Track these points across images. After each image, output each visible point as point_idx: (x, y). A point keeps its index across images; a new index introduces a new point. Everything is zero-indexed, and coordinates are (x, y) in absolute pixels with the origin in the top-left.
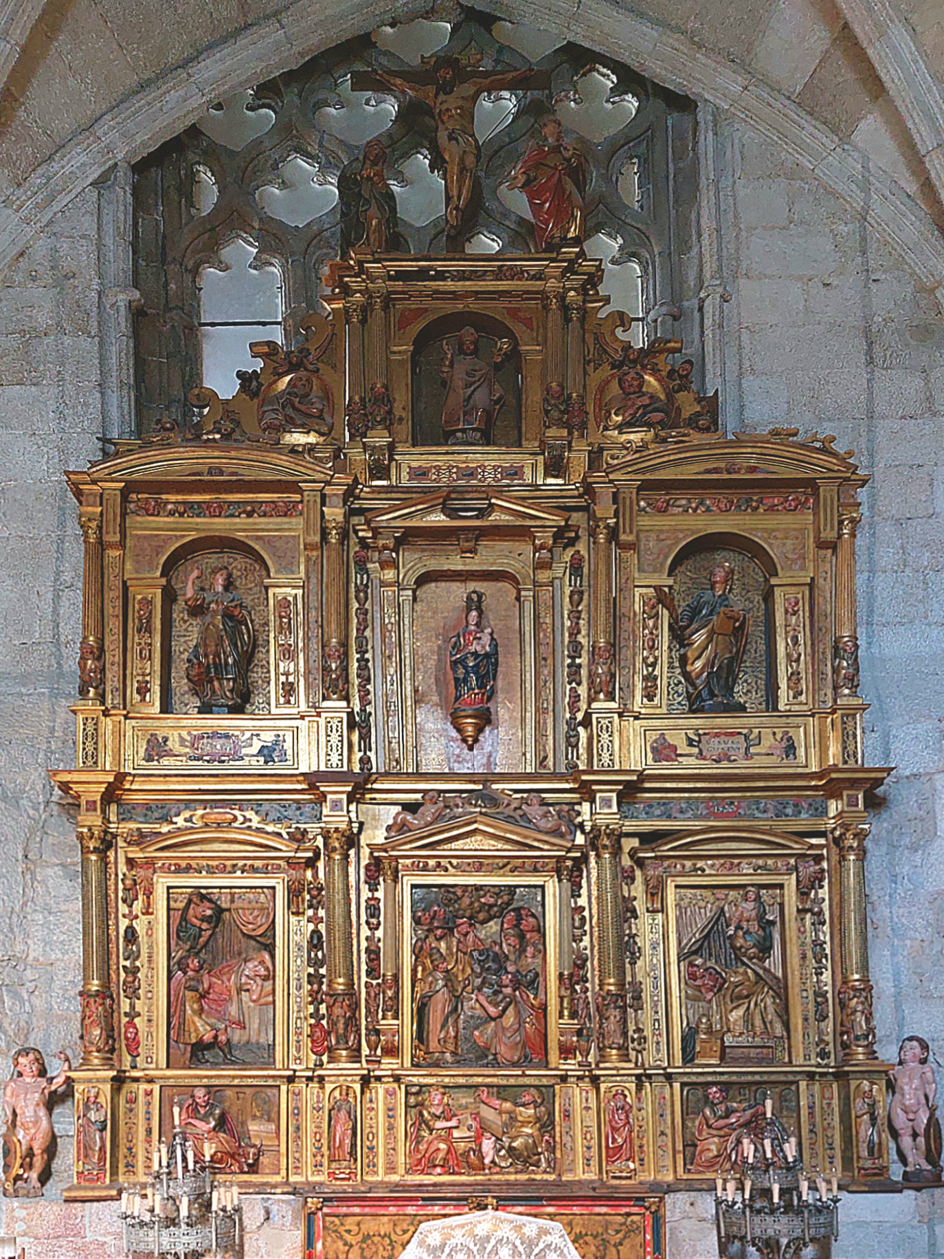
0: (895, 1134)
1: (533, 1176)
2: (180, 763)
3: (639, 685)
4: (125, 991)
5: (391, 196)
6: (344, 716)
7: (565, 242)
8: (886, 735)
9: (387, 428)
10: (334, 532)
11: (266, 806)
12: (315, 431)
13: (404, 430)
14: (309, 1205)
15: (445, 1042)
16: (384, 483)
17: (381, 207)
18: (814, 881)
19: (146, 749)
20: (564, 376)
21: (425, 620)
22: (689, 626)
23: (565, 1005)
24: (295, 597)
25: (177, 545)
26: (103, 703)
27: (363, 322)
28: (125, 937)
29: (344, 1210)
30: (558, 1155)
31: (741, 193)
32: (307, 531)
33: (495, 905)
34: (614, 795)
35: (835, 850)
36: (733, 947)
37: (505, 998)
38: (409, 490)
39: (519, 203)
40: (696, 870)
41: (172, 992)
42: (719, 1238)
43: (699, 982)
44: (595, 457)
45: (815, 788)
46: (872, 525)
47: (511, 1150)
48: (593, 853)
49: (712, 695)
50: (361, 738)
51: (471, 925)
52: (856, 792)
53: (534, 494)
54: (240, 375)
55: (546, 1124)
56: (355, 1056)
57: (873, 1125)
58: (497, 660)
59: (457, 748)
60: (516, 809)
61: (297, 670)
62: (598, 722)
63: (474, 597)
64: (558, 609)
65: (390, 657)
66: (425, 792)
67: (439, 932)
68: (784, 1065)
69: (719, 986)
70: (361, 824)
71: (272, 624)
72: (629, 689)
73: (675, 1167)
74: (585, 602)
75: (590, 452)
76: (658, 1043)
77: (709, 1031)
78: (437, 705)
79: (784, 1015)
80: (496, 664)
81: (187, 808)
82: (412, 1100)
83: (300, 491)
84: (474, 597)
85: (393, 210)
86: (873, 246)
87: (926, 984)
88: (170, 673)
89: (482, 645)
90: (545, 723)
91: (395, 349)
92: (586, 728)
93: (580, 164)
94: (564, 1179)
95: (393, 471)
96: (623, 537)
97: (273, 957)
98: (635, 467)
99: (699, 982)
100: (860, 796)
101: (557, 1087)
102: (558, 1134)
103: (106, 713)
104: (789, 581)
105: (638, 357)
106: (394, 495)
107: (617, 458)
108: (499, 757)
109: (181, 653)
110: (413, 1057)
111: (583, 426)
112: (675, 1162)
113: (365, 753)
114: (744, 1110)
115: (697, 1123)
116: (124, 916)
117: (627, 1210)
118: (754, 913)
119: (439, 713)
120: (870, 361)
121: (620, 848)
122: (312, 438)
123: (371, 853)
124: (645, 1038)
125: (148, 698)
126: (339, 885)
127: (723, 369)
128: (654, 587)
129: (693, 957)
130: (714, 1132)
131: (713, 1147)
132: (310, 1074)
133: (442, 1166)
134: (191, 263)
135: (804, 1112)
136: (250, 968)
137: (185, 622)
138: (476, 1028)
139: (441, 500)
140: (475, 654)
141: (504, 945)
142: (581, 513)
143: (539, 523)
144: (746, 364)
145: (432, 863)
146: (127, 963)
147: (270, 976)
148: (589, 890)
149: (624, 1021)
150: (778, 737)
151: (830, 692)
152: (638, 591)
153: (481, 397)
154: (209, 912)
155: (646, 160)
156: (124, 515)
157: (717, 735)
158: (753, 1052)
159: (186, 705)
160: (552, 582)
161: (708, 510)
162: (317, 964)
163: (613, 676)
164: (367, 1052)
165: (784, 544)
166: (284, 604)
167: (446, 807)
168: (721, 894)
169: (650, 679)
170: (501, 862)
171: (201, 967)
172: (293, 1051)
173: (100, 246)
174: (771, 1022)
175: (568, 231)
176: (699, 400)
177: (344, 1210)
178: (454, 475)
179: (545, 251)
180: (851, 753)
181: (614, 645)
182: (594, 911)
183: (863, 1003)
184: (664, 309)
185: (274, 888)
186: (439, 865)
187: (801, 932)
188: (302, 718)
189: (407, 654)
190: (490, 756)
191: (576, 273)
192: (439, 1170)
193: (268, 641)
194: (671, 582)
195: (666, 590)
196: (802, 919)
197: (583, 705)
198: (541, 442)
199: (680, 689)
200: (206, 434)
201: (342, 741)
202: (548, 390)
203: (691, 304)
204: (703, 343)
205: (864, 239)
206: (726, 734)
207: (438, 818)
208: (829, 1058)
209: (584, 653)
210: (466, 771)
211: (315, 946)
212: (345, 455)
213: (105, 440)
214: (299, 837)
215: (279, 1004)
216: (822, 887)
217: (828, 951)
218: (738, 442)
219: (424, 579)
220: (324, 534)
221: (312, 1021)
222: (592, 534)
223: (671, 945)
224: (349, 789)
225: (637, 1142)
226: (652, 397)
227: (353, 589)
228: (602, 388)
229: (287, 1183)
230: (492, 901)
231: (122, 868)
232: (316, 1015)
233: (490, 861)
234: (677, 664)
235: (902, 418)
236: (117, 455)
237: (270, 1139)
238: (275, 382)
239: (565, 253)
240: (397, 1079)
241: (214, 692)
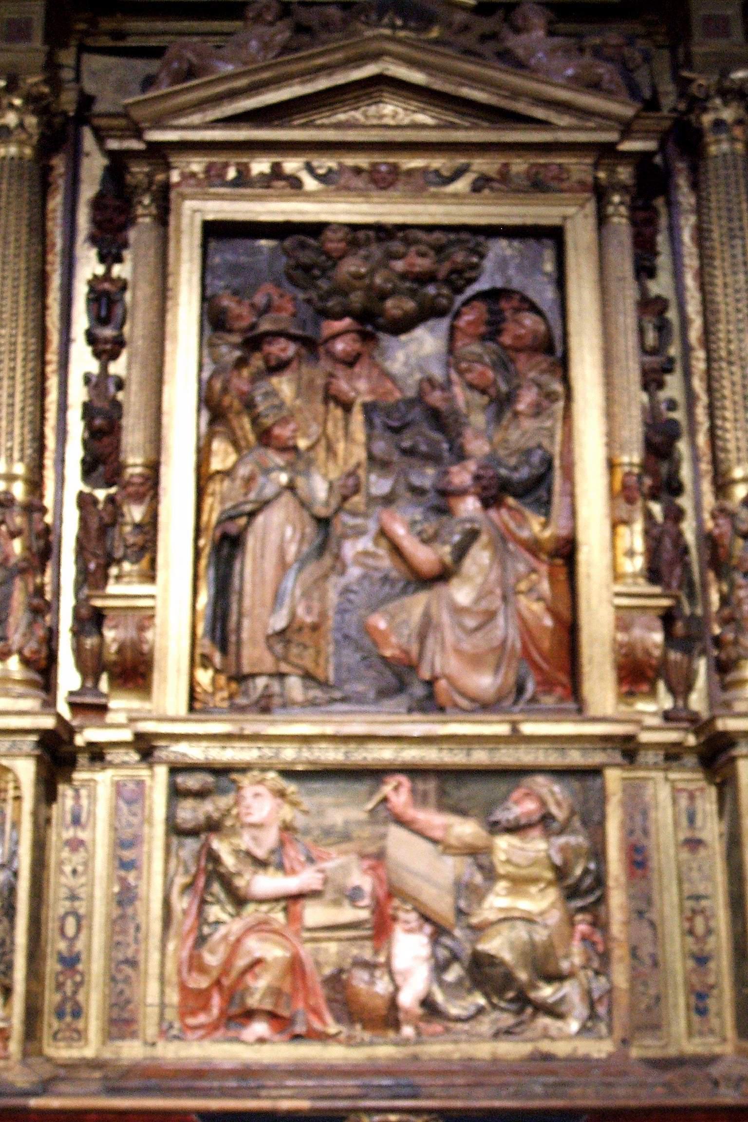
1: (546, 1046)
133: (272, 1016)
138: (374, 608)
192: (260, 1028)
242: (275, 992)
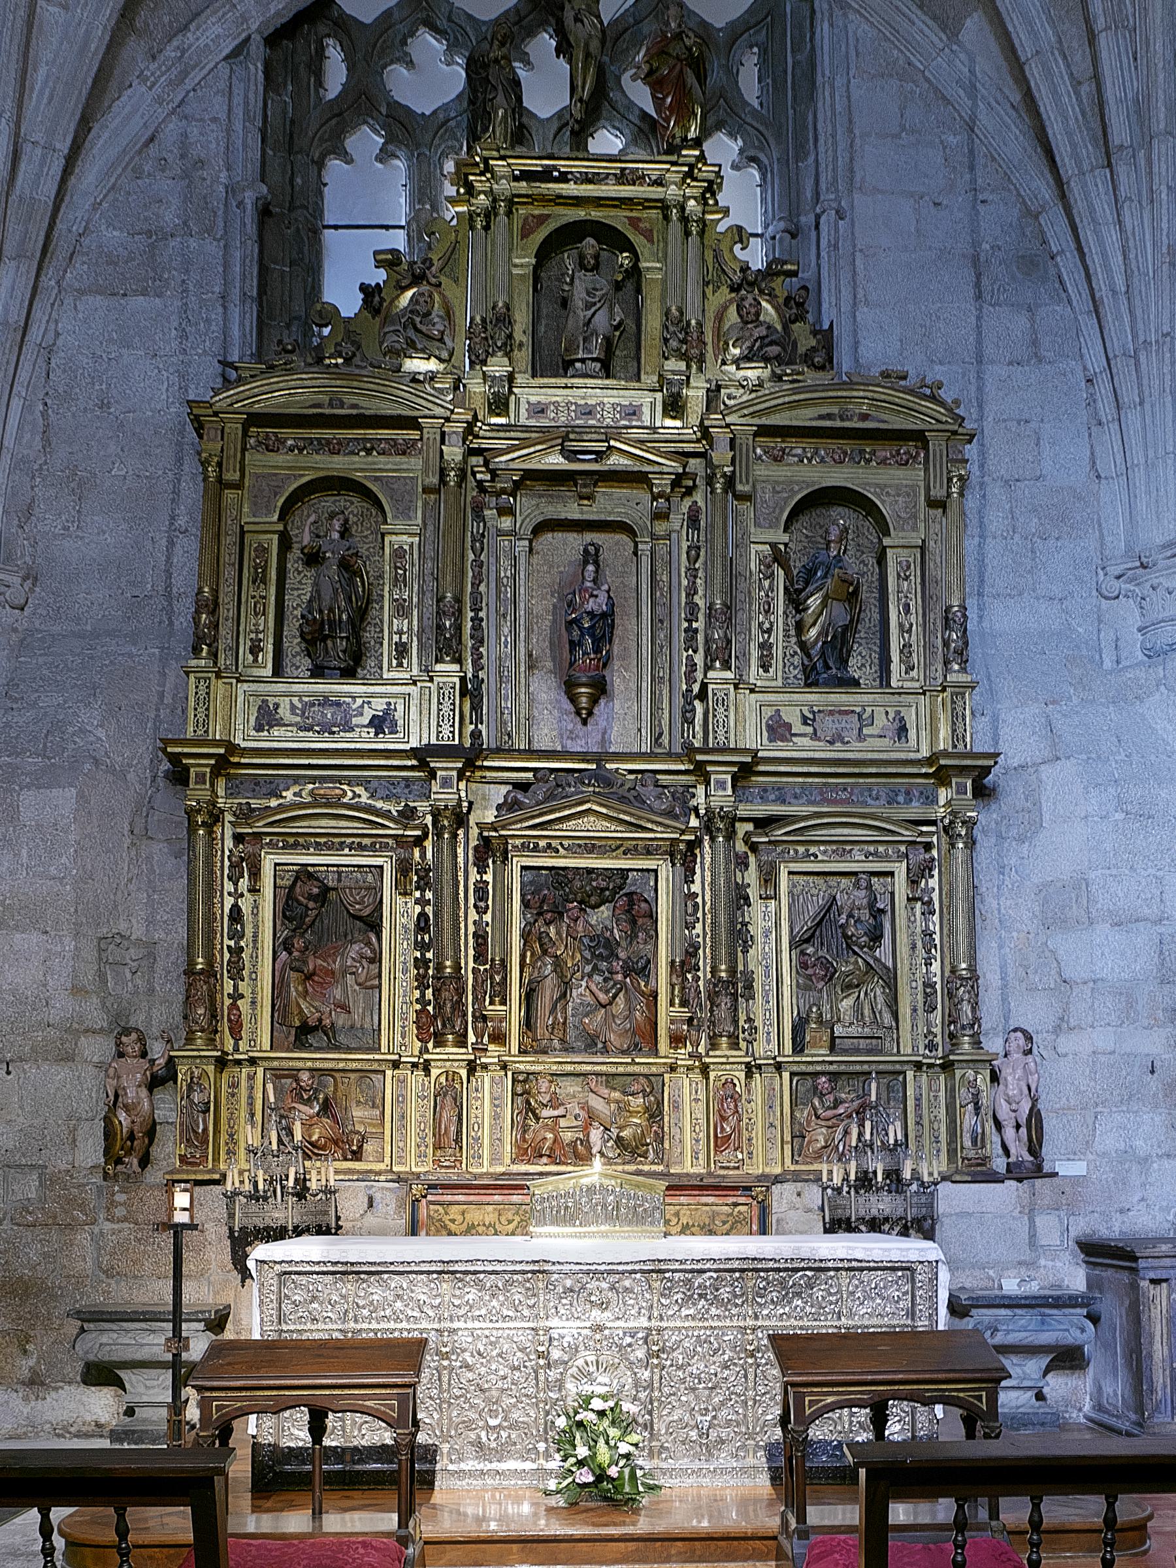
1: (640, 1167)
2: (290, 734)
3: (755, 653)
4: (228, 972)
6: (457, 680)
7: (686, 143)
8: (995, 719)
9: (508, 355)
10: (452, 474)
11: (375, 784)
12: (436, 357)
13: (523, 356)
14: (414, 1192)
15: (553, 1028)
16: (502, 420)
17: (507, 98)
18: (924, 870)
19: (257, 718)
20: (684, 298)
21: (541, 574)
22: (804, 589)
23: (676, 992)
25: (295, 486)
26: (215, 663)
27: (487, 228)
28: (231, 917)
29: (449, 1198)
30: (666, 1145)
31: (855, 94)
33: (608, 889)
34: (729, 777)
36: (845, 936)
37: (615, 984)
38: (527, 429)
39: (641, 96)
40: (809, 856)
41: (277, 973)
42: (825, 1224)
43: (810, 971)
44: (713, 393)
46: (982, 484)
47: (619, 1140)
48: (707, 838)
50: (473, 708)
51: (581, 909)
52: (964, 780)
54: (364, 288)
56: (461, 1041)
57: (977, 1114)
58: (613, 621)
59: (571, 723)
60: (630, 789)
61: (410, 629)
64: (674, 565)
65: (504, 616)
66: (535, 770)
67: (549, 916)
68: (892, 1055)
70: (471, 804)
71: (387, 576)
72: (745, 655)
73: (783, 1159)
74: (701, 560)
75: (708, 390)
76: (768, 1033)
77: (820, 1021)
78: (551, 672)
80: (612, 626)
81: (296, 783)
83: (418, 427)
84: (591, 549)
85: (519, 99)
86: (980, 161)
87: (1031, 976)
88: (282, 631)
89: (597, 604)
90: (661, 694)
91: (517, 261)
92: (702, 701)
93: (701, 53)
94: (672, 1171)
95: (512, 406)
96: (739, 487)
97: (379, 939)
98: (751, 410)
99: (810, 971)
101: (666, 1076)
102: (666, 1124)
103: (218, 676)
104: (902, 542)
105: (756, 279)
106: (512, 434)
107: (735, 398)
108: (614, 734)
109: (295, 609)
111: (701, 360)
112: (783, 1153)
113: (476, 726)
114: (852, 1101)
116: (230, 894)
117: (734, 1200)
118: (865, 901)
119: (553, 681)
120: (979, 296)
121: (734, 832)
122: (433, 365)
123: (481, 834)
124: (756, 1028)
125: (260, 659)
126: (447, 864)
127: (838, 299)
128: (770, 544)
129: (805, 946)
130: (823, 1123)
131: (821, 1138)
132: (416, 1060)
133: (549, 1156)
134: (317, 155)
135: (911, 1103)
136: (354, 950)
137: (299, 573)
138: (587, 1015)
139: (560, 441)
140: (591, 614)
141: (615, 931)
142: (698, 460)
143: (657, 469)
144: (860, 296)
145: (542, 843)
146: (232, 943)
147: (376, 959)
148: (703, 877)
149: (735, 1009)
150: (891, 716)
151: (940, 667)
153: (601, 321)
154: (316, 891)
155: (766, 50)
156: (244, 450)
157: (831, 713)
158: (863, 1043)
160: (669, 535)
161: (822, 461)
163: (729, 642)
164: (474, 1040)
165: (896, 502)
166: (399, 553)
167: (558, 786)
168: (833, 881)
169: (765, 646)
170: (614, 844)
171: (306, 948)
172: (398, 1038)
173: (229, 131)
174: (880, 1013)
175: (689, 130)
176: (815, 333)
177: (449, 1198)
178: (573, 414)
179: (667, 153)
181: (729, 608)
182: (708, 897)
183: (969, 992)
184: (782, 225)
185: (381, 867)
186: (549, 846)
188: (415, 683)
189: (522, 613)
190: (604, 733)
191: (695, 179)
192: (545, 1160)
193: (382, 596)
194: (785, 538)
195: (782, 547)
197: (699, 675)
198: (660, 376)
200: (329, 358)
201: (454, 710)
202: (667, 313)
203: (807, 220)
204: (819, 266)
205: (971, 151)
206: (841, 712)
207: (550, 797)
209: (701, 617)
210: (579, 749)
211: (422, 929)
212: (464, 386)
213: (225, 363)
214: (408, 814)
215: (385, 987)
217: (937, 942)
221: (418, 1007)
222: (710, 481)
223: (783, 933)
224: (460, 765)
225: (745, 1134)
226: (769, 328)
227: (469, 539)
228: (720, 317)
229: (391, 1171)
230: (603, 884)
231: (229, 843)
232: (422, 1000)
233: (603, 843)
234: (793, 632)
235: (1010, 363)
236: (240, 381)
237: (374, 1126)
238: (398, 296)
239: (685, 156)
240: (504, 1067)
241: (327, 652)
242: (551, 1149)
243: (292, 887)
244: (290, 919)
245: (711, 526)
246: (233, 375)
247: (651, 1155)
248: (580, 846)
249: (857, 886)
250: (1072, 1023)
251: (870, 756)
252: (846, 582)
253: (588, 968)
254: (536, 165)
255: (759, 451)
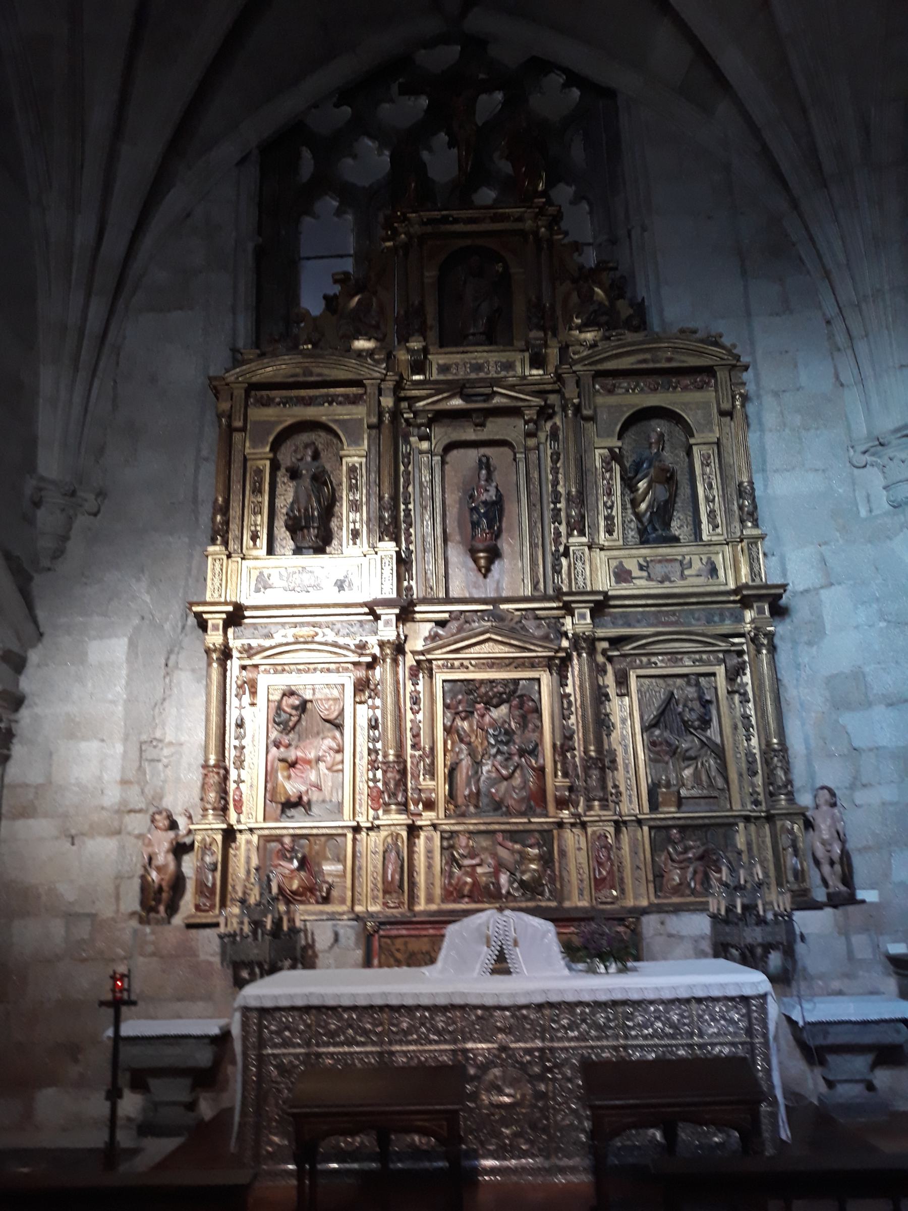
0: (817, 863)
3: (602, 523)
5: (424, 165)
11: (338, 626)
13: (433, 335)
24: (361, 464)
29: (394, 932)
32: (369, 415)
33: (505, 693)
35: (752, 646)
38: (437, 382)
44: (564, 350)
45: (734, 602)
47: (522, 883)
49: (655, 530)
53: (523, 384)
54: (325, 297)
55: (546, 860)
60: (517, 623)
62: (574, 553)
63: (484, 460)
65: (426, 508)
66: (450, 612)
69: (674, 751)
70: (406, 637)
72: (595, 527)
76: (630, 796)
79: (723, 771)
82: (445, 844)
84: (484, 460)
97: (342, 734)
99: (658, 749)
100: (766, 607)
106: (427, 386)
110: (445, 809)
115: (663, 858)
118: (695, 695)
119: (461, 548)
129: (653, 730)
133: (469, 896)
140: (485, 503)
143: (526, 404)
145: (457, 663)
150: (704, 561)
152: (597, 452)
154: (297, 702)
159: (284, 548)
161: (642, 390)
162: (375, 740)
163: (583, 517)
166: (352, 470)
167: (467, 622)
168: (670, 681)
169: (609, 518)
170: (507, 661)
176: (631, 305)
180: (757, 572)
186: (462, 665)
187: (731, 708)
194: (619, 444)
195: (617, 450)
196: (732, 699)
197: (563, 540)
199: (633, 525)
200: (303, 344)
207: (460, 630)
208: (761, 805)
209: (563, 500)
216: (745, 674)
218: (659, 340)
219: (449, 448)
220: (380, 415)
222: (564, 409)
230: (502, 690)
234: (629, 506)
240: (435, 826)
242: (471, 891)
243: (280, 702)
244: (278, 724)
245: (566, 439)
246: (239, 357)
247: (547, 894)
248: (483, 664)
249: (688, 683)
250: (864, 781)
251: (691, 590)
252: (665, 470)
253: (494, 751)
254: (436, 214)
255: (597, 387)
